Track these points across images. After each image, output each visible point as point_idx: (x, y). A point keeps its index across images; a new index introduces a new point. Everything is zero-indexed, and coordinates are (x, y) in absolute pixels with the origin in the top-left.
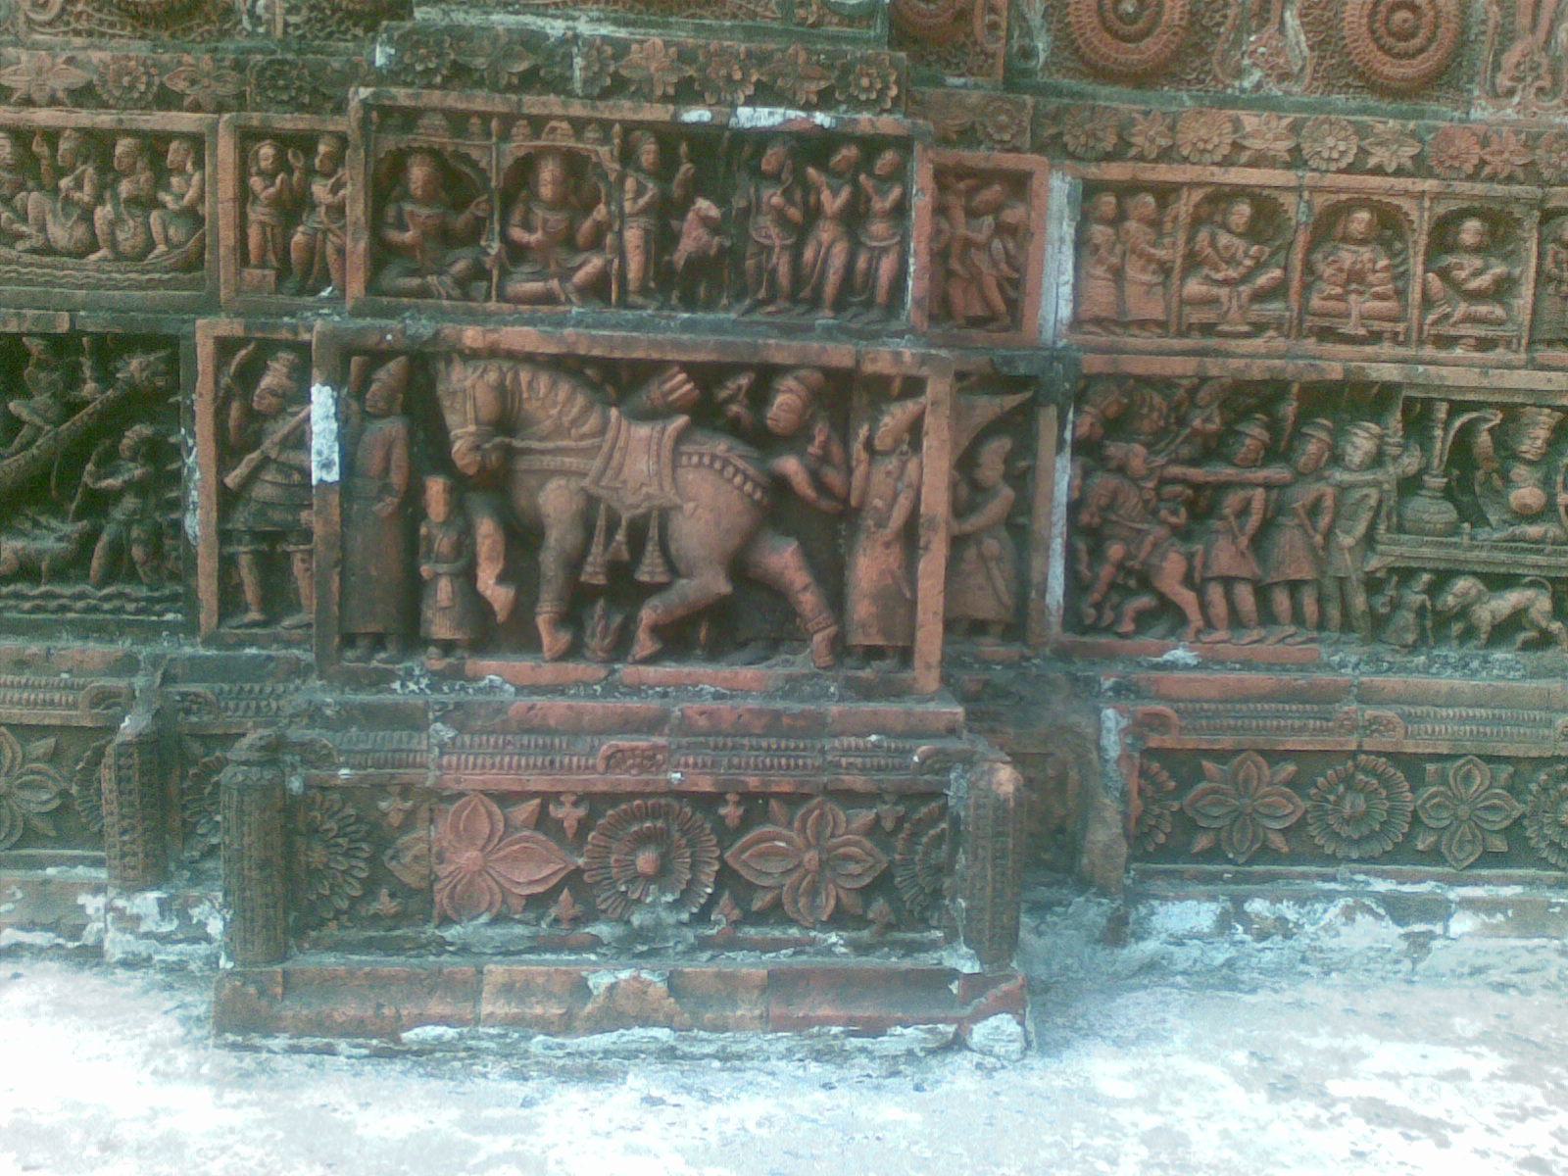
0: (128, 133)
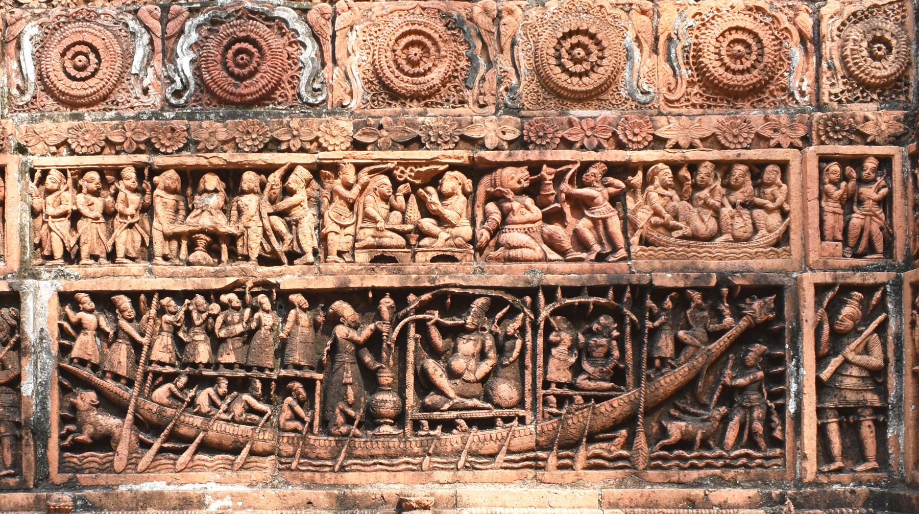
0: (742, 162)
